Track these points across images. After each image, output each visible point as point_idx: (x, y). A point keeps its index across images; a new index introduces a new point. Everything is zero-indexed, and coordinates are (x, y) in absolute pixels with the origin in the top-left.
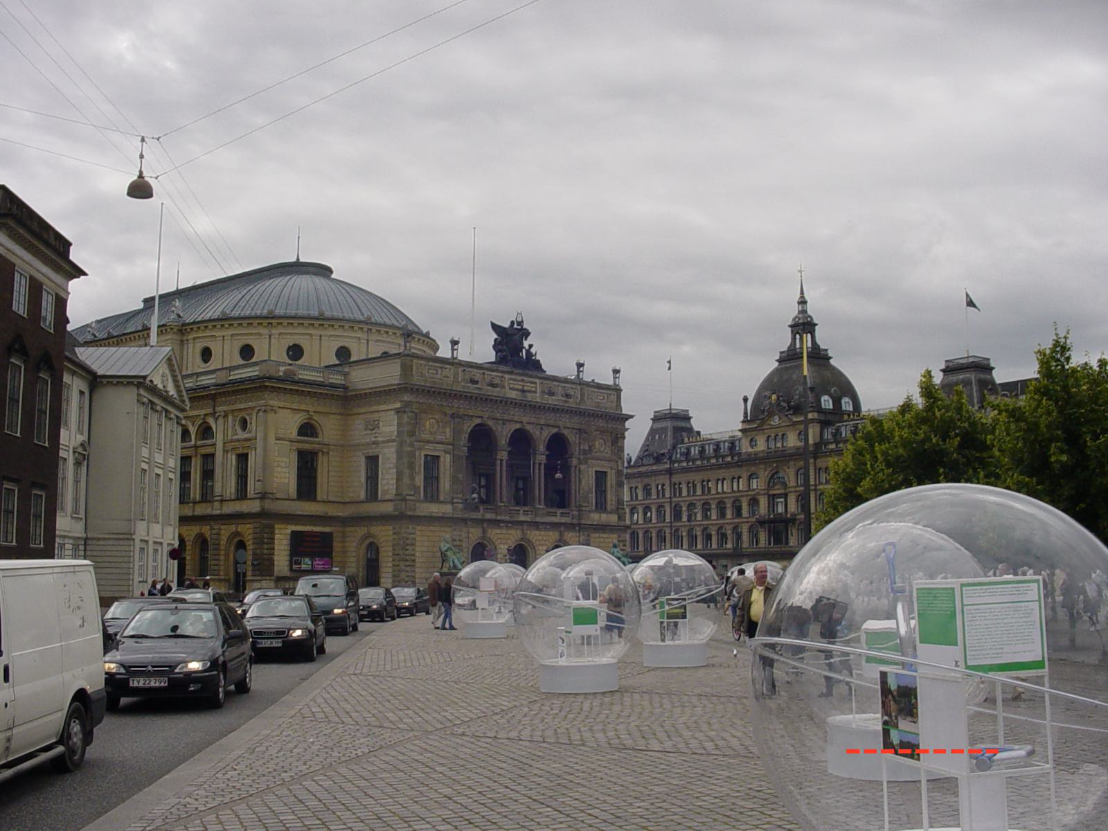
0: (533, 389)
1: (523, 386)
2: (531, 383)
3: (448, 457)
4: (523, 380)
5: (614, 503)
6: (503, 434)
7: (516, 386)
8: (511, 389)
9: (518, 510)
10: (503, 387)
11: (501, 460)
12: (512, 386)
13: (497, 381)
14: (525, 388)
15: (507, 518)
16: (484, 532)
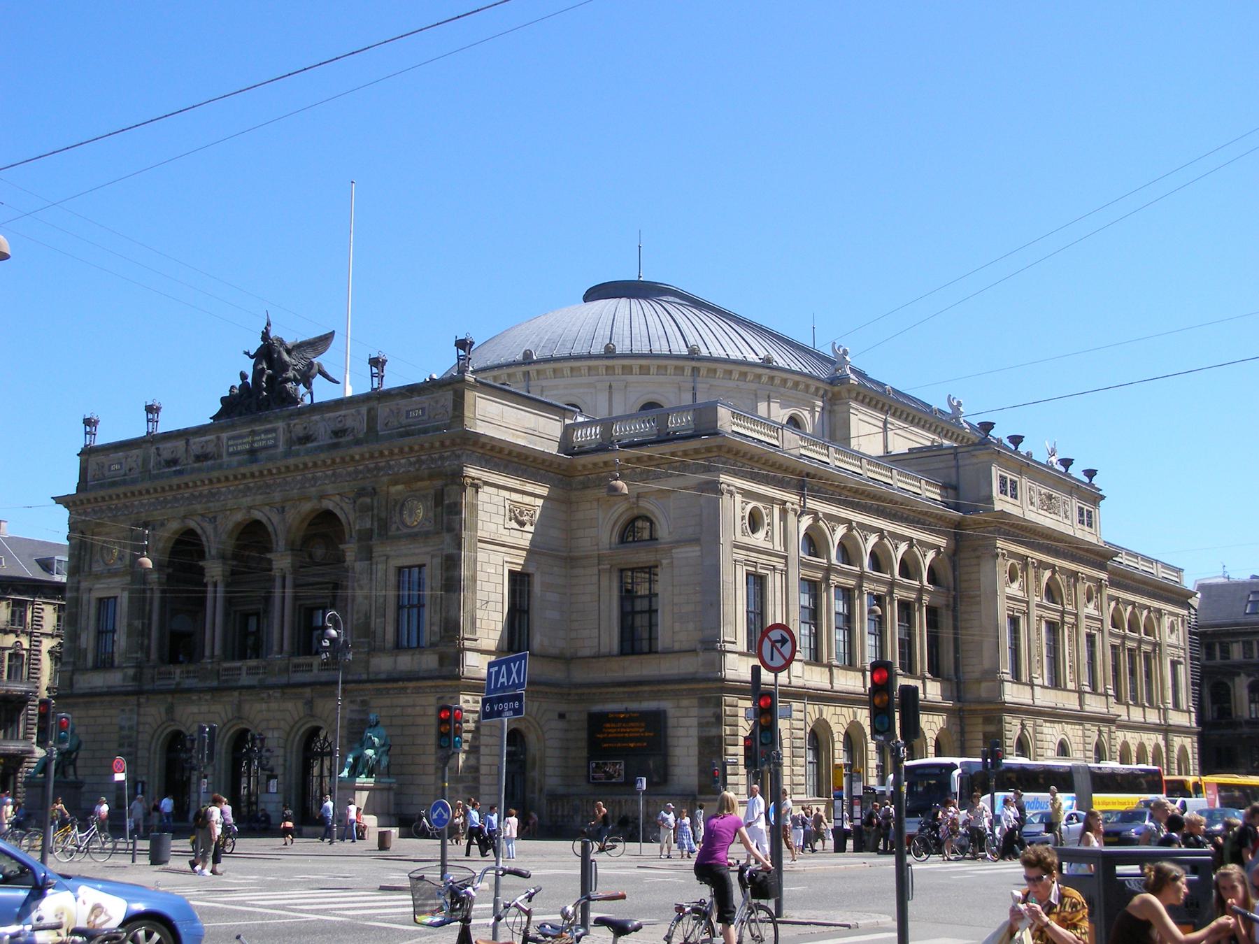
0: (271, 442)
1: (253, 442)
2: (267, 432)
3: (126, 595)
4: (254, 433)
5: (436, 629)
6: (217, 538)
7: (240, 448)
8: (231, 454)
9: (240, 669)
10: (220, 456)
11: (215, 585)
12: (231, 449)
13: (211, 449)
14: (256, 445)
15: (215, 684)
16: (170, 710)
